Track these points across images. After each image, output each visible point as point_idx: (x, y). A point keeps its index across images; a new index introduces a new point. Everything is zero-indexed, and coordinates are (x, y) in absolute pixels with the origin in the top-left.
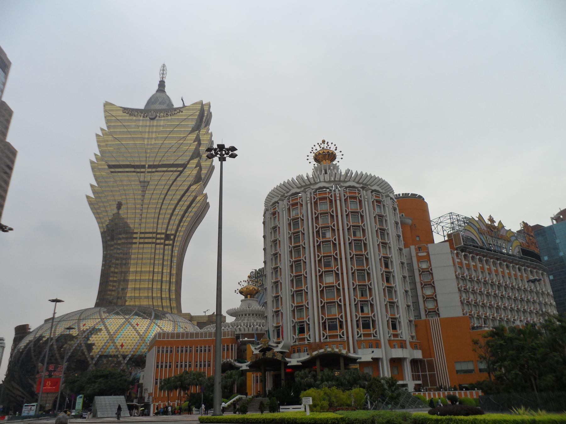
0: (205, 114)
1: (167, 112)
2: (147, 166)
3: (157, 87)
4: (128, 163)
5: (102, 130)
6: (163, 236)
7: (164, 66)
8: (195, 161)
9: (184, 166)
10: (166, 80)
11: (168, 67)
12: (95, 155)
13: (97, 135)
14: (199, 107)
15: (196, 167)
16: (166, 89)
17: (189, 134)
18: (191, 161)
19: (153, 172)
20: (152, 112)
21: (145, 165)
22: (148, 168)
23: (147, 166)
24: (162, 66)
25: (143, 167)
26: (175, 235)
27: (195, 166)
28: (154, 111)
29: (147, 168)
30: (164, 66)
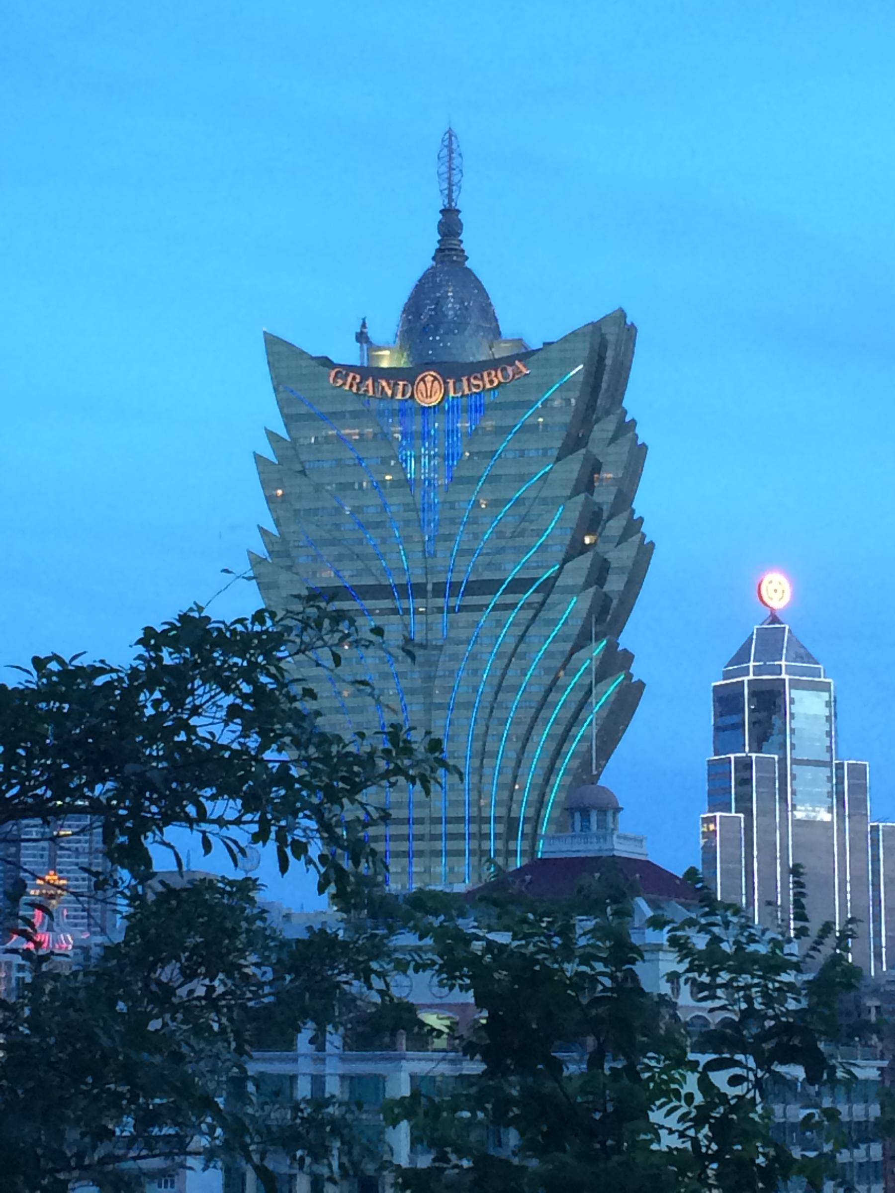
0: (608, 362)
1: (475, 378)
2: (430, 587)
3: (431, 241)
4: (372, 582)
5: (272, 436)
6: (501, 828)
7: (450, 134)
8: (584, 562)
9: (549, 586)
10: (461, 202)
11: (466, 142)
12: (263, 532)
13: (258, 458)
14: (583, 348)
15: (587, 585)
16: (469, 241)
17: (558, 459)
18: (569, 565)
19: (451, 610)
20: (429, 379)
21: (426, 584)
22: (434, 596)
23: (430, 587)
24: (443, 141)
25: (418, 590)
26: (536, 821)
27: (581, 581)
28: (435, 378)
29: (430, 595)
30: (450, 134)
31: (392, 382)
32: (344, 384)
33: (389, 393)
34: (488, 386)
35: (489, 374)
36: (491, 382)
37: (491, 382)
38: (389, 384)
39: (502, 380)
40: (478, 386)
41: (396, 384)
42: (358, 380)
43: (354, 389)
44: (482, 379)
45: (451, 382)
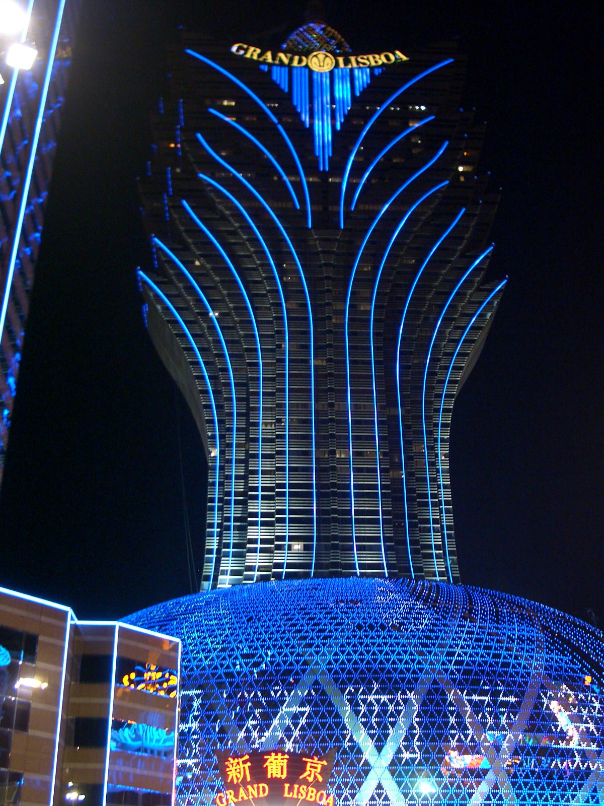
1: (362, 58)
31: (289, 55)
32: (245, 53)
33: (286, 61)
34: (373, 64)
35: (374, 58)
36: (376, 62)
37: (376, 62)
38: (286, 56)
39: (385, 61)
40: (364, 64)
41: (291, 60)
42: (259, 51)
43: (255, 57)
44: (368, 59)
45: (341, 60)
